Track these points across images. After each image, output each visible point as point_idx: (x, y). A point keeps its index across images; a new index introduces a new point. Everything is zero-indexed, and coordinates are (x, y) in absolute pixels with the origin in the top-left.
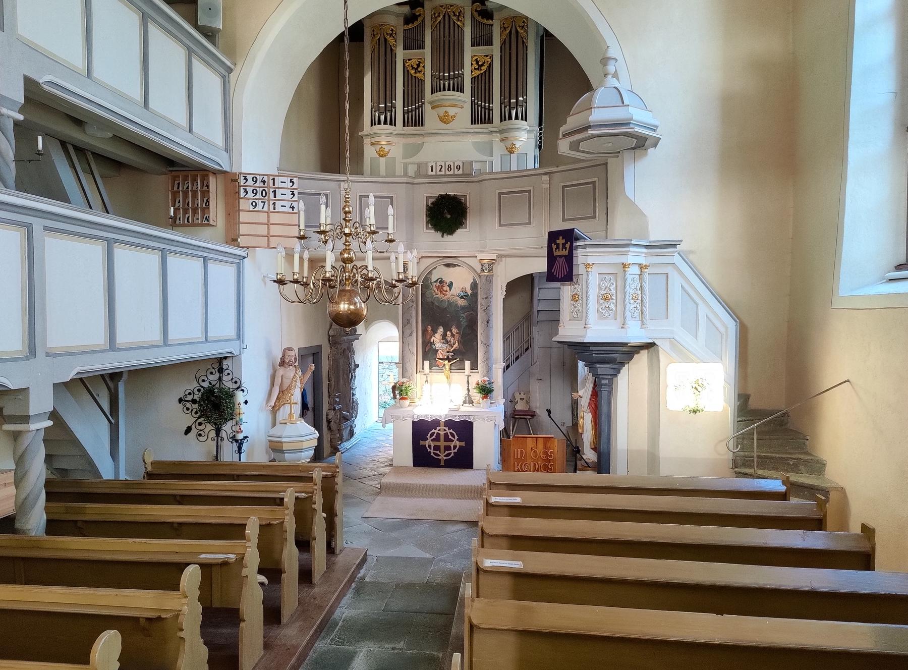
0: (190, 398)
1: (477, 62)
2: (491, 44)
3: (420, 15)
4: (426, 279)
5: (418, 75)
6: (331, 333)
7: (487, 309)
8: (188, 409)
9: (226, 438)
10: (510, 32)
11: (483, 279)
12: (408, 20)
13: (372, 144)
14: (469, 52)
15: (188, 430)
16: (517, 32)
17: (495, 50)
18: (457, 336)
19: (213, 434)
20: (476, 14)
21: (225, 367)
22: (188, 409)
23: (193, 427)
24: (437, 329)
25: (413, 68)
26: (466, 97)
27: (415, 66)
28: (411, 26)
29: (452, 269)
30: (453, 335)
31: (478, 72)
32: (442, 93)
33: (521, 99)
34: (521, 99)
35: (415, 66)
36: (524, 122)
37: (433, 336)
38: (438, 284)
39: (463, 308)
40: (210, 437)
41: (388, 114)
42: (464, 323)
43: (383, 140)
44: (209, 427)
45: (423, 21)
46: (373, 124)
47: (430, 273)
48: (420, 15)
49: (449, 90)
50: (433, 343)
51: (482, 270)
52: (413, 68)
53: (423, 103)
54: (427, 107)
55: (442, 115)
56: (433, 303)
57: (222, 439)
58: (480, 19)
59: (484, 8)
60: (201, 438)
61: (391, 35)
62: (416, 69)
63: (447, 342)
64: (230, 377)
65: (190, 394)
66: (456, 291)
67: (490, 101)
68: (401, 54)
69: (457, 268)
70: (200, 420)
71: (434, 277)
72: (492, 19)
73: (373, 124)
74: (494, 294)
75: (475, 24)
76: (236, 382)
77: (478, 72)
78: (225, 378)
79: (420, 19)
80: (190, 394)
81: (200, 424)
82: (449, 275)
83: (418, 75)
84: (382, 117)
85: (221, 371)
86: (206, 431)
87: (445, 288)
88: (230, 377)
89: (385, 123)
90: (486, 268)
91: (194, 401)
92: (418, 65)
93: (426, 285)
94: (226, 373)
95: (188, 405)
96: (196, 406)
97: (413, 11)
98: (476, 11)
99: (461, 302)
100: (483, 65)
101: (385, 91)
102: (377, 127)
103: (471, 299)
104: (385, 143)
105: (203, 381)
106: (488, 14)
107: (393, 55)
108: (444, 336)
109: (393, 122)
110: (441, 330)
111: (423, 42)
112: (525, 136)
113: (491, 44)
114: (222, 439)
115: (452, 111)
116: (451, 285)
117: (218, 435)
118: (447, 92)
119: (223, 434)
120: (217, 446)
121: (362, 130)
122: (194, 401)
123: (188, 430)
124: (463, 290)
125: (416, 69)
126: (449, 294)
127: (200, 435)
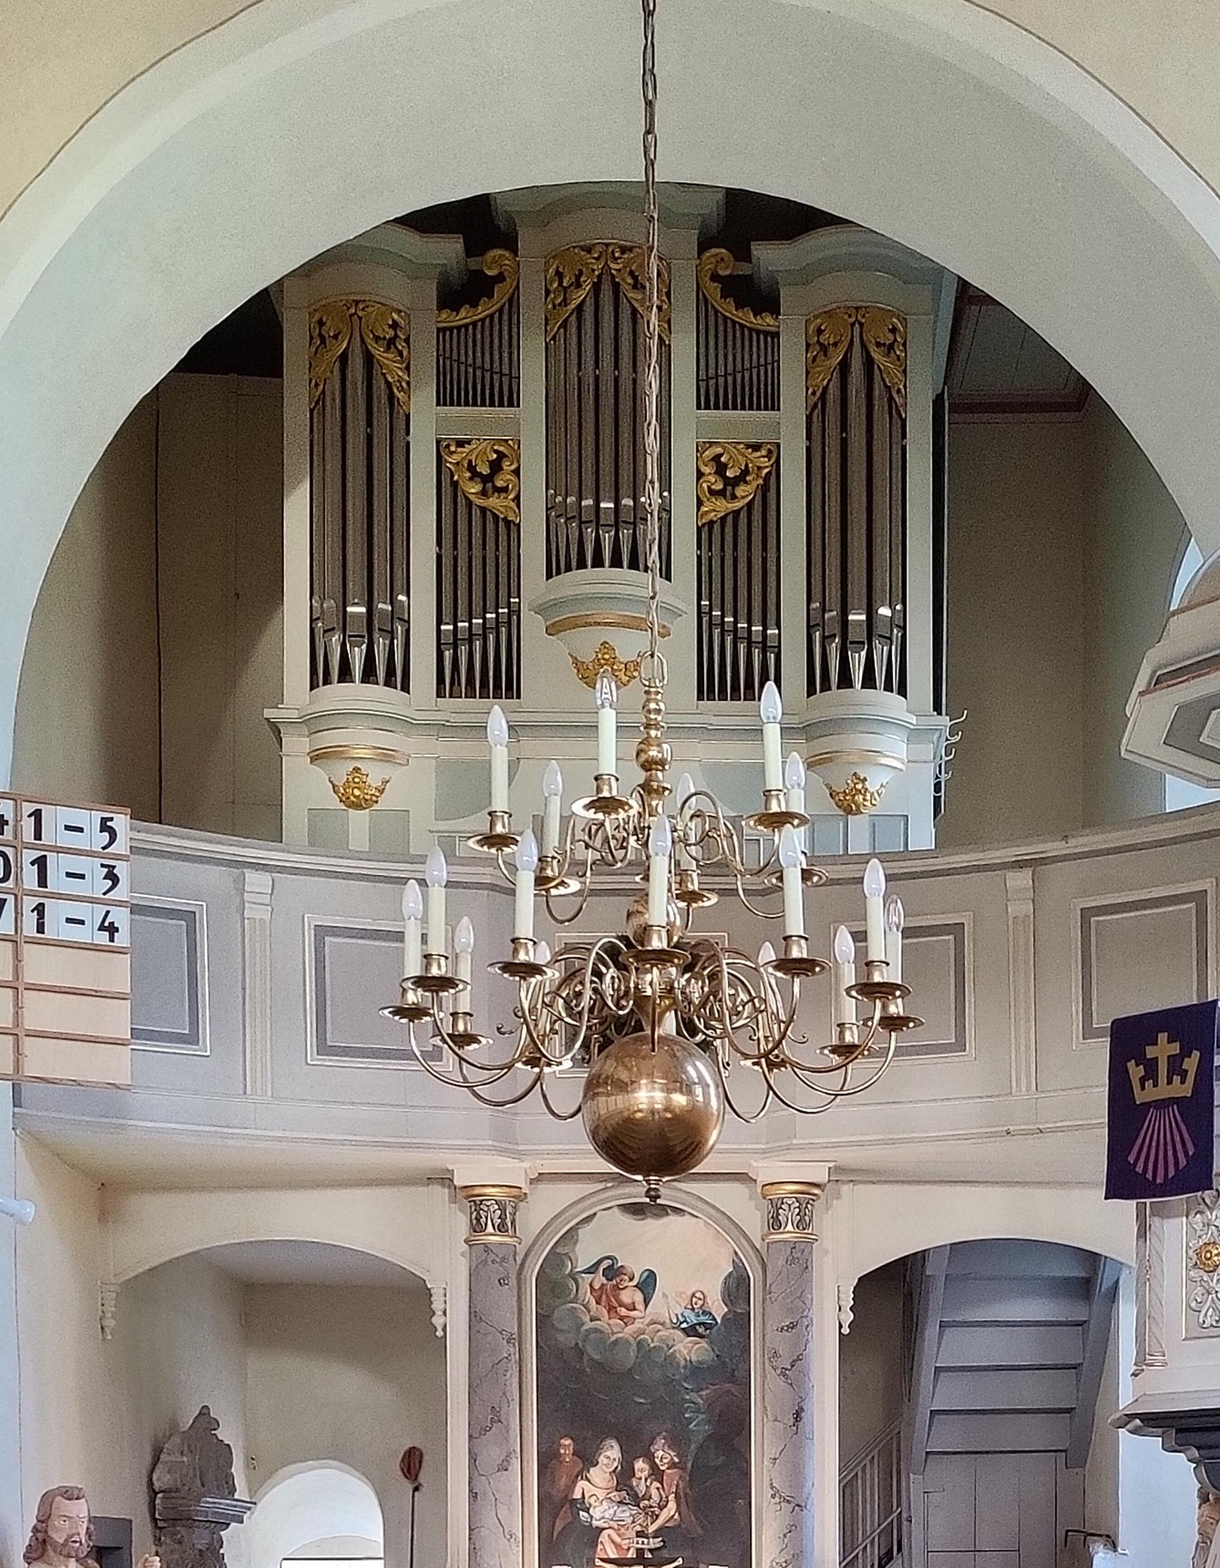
1: (721, 469)
2: (772, 403)
3: (500, 278)
4: (556, 1259)
5: (494, 502)
6: (161, 1479)
7: (794, 1370)
10: (844, 366)
11: (777, 1263)
12: (458, 292)
13: (317, 757)
14: (691, 428)
16: (869, 363)
17: (789, 424)
18: (672, 1476)
20: (714, 290)
24: (598, 1449)
25: (475, 474)
26: (682, 591)
27: (484, 470)
28: (465, 315)
29: (651, 1225)
30: (656, 1474)
31: (724, 506)
32: (590, 573)
33: (885, 611)
34: (885, 611)
35: (484, 470)
36: (894, 697)
37: (581, 1474)
38: (600, 1280)
39: (695, 1370)
41: (381, 644)
42: (699, 1427)
43: (360, 739)
45: (513, 301)
46: (319, 677)
47: (570, 1236)
48: (500, 278)
49: (616, 562)
50: (582, 1505)
51: (775, 1223)
52: (475, 474)
53: (515, 612)
54: (532, 626)
55: (588, 657)
56: (580, 1352)
58: (728, 308)
59: (744, 269)
61: (391, 342)
62: (486, 479)
63: (636, 1499)
66: (668, 1304)
67: (770, 613)
68: (426, 419)
69: (672, 1218)
71: (585, 1254)
72: (776, 312)
73: (319, 677)
74: (814, 1313)
75: (710, 325)
77: (724, 506)
79: (501, 294)
82: (645, 1245)
83: (494, 502)
84: (357, 657)
87: (625, 1297)
89: (369, 675)
90: (789, 1216)
92: (496, 466)
93: (554, 1283)
97: (474, 263)
98: (715, 277)
99: (688, 1349)
100: (741, 479)
101: (363, 553)
102: (337, 695)
103: (728, 1333)
104: (361, 748)
106: (763, 298)
107: (400, 423)
108: (624, 1477)
109: (397, 677)
110: (611, 1454)
111: (514, 378)
112: (899, 749)
113: (772, 403)
115: (628, 645)
116: (648, 1284)
118: (607, 572)
121: (277, 699)
124: (696, 1302)
125: (486, 479)
126: (641, 1318)
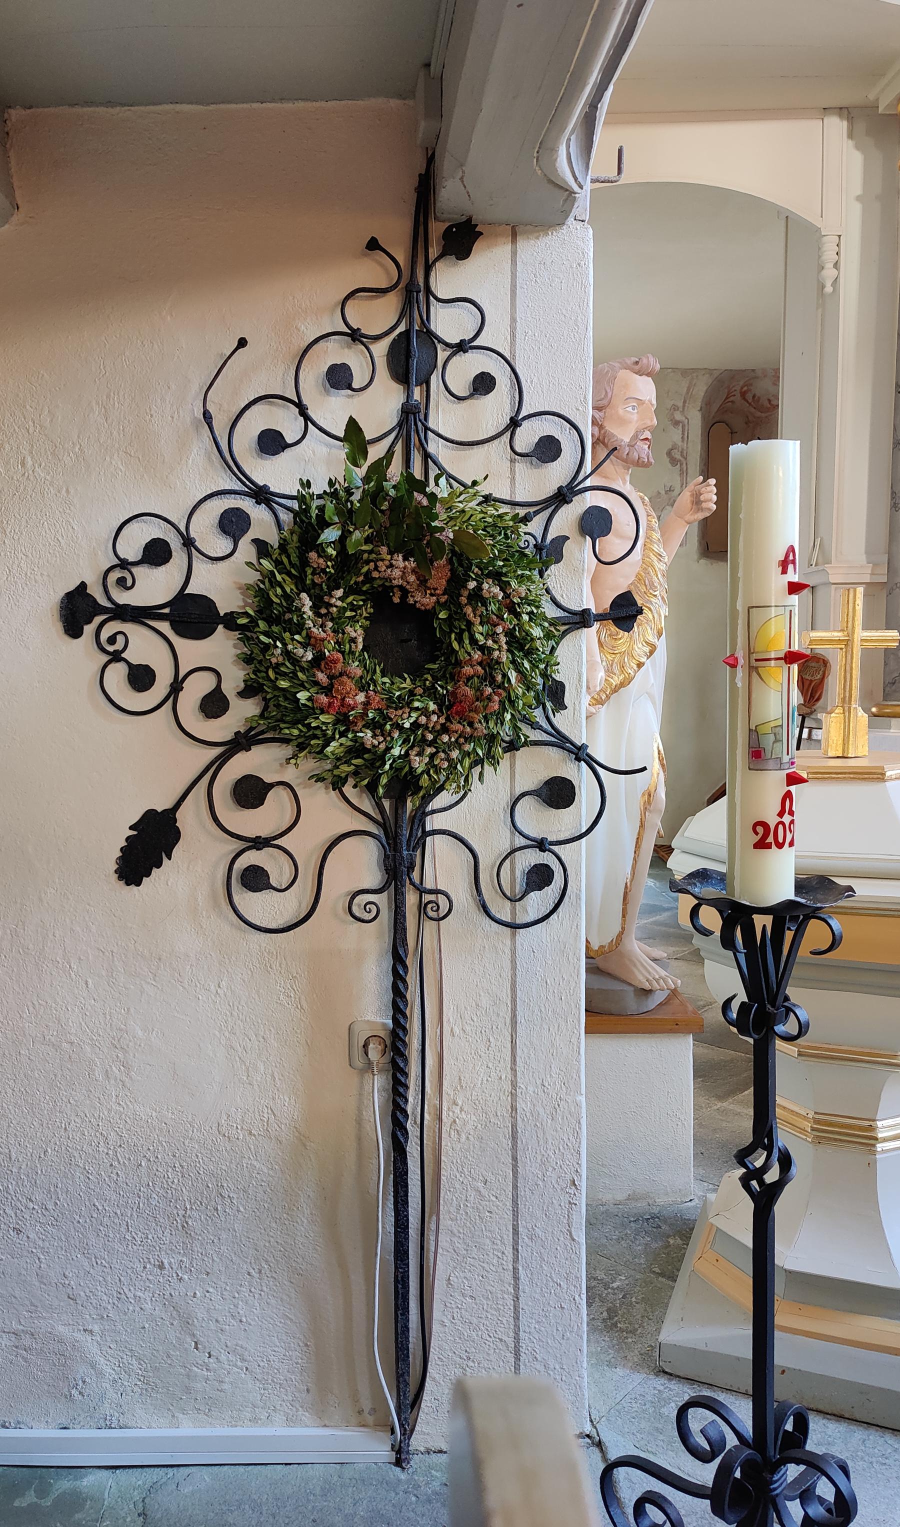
0: (154, 587)
8: (141, 678)
9: (462, 894)
15: (148, 846)
19: (360, 863)
21: (448, 324)
22: (141, 678)
23: (190, 819)
40: (337, 885)
44: (327, 813)
57: (435, 906)
60: (255, 905)
64: (494, 409)
65: (156, 553)
70: (260, 761)
76: (548, 450)
78: (445, 417)
80: (156, 553)
81: (250, 792)
85: (413, 356)
86: (304, 843)
88: (494, 409)
91: (191, 615)
94: (461, 371)
95: (144, 645)
96: (220, 650)
105: (272, 443)
114: (435, 906)
117: (400, 860)
119: (442, 865)
120: (398, 959)
122: (191, 615)
123: (148, 846)
127: (255, 879)
